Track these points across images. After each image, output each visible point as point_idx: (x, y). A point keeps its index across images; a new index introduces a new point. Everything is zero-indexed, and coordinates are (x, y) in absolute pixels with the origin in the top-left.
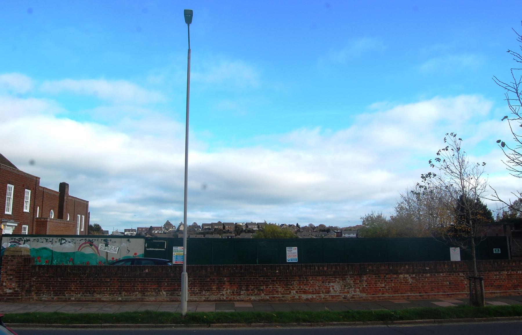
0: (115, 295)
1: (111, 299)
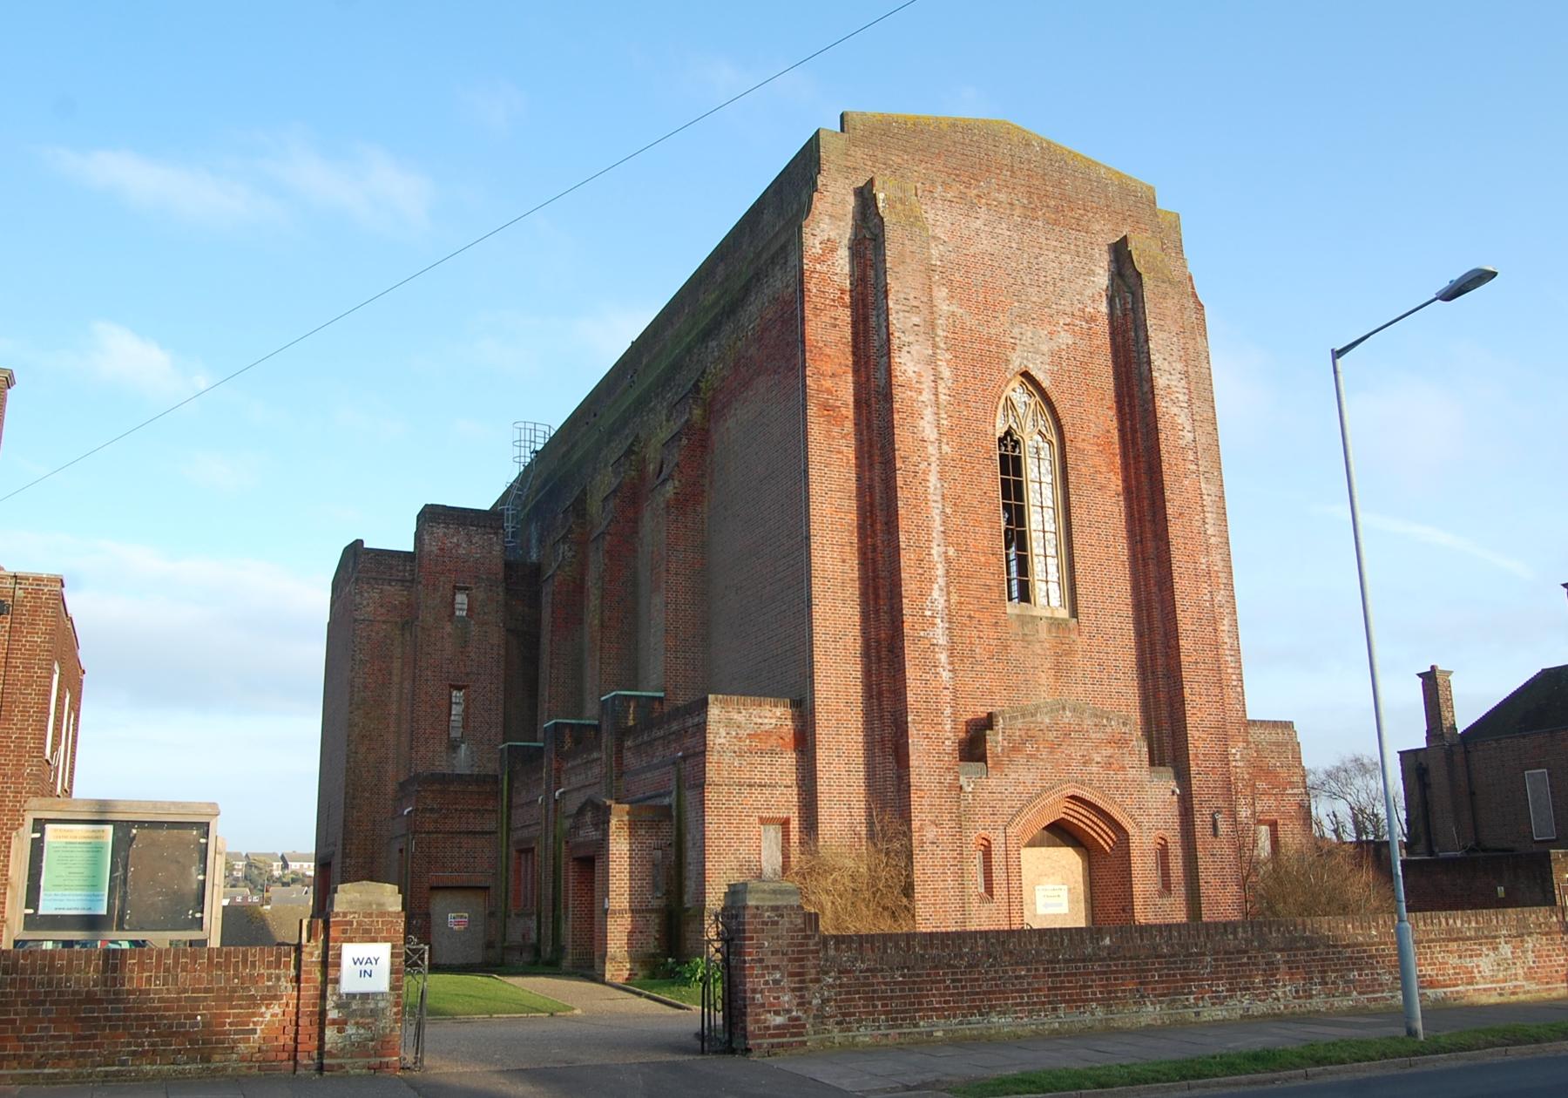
0: (1043, 1014)
1: (1034, 1027)
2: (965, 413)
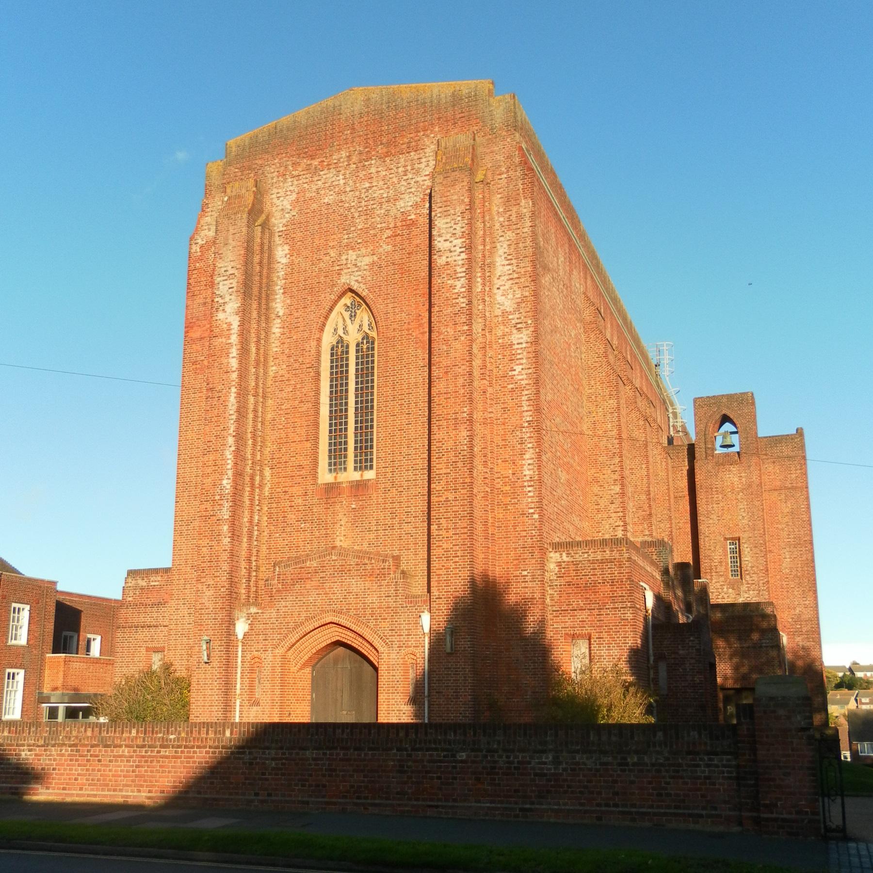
2: (294, 338)
